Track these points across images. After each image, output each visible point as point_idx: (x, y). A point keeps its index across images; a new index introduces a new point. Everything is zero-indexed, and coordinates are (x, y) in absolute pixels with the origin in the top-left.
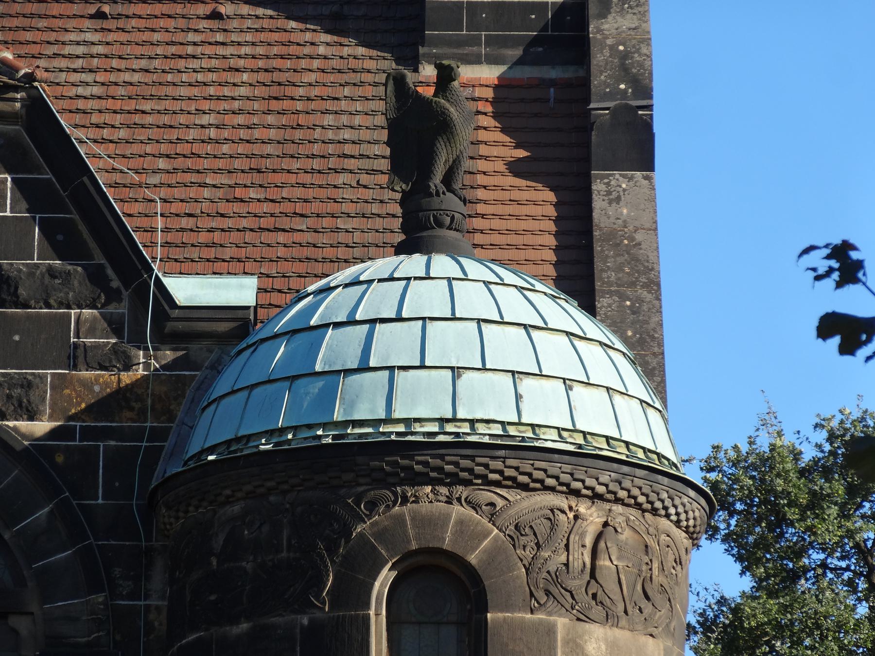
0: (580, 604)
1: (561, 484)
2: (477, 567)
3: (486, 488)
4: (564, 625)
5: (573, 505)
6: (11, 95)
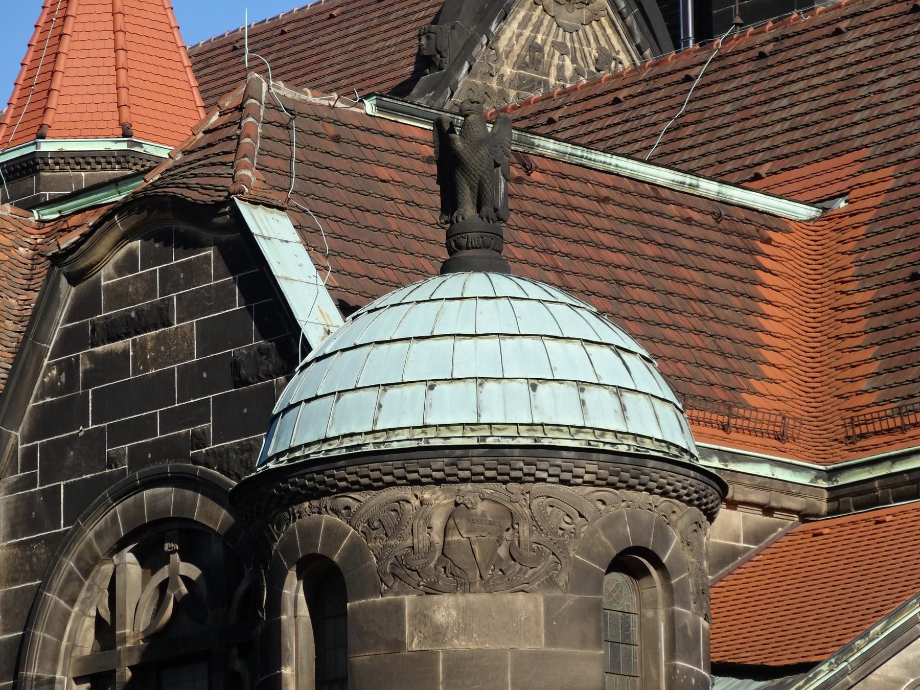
0: (425, 580)
1: (399, 478)
2: (339, 565)
3: (343, 494)
4: (411, 601)
5: (418, 493)
6: (222, 210)
